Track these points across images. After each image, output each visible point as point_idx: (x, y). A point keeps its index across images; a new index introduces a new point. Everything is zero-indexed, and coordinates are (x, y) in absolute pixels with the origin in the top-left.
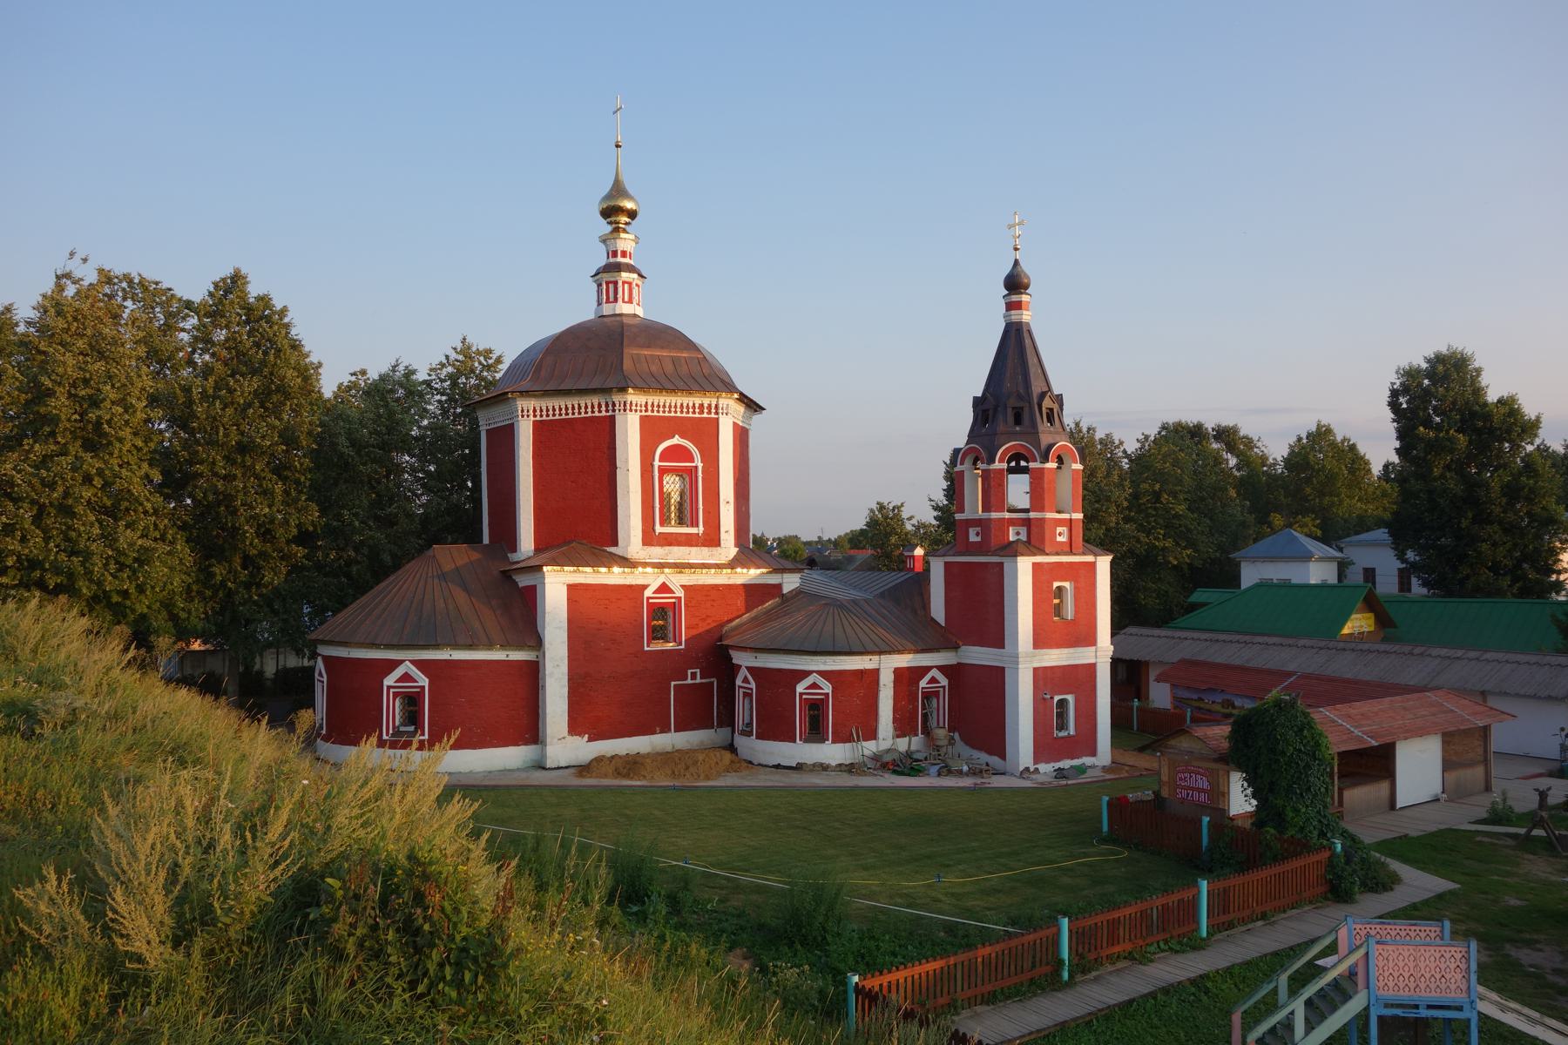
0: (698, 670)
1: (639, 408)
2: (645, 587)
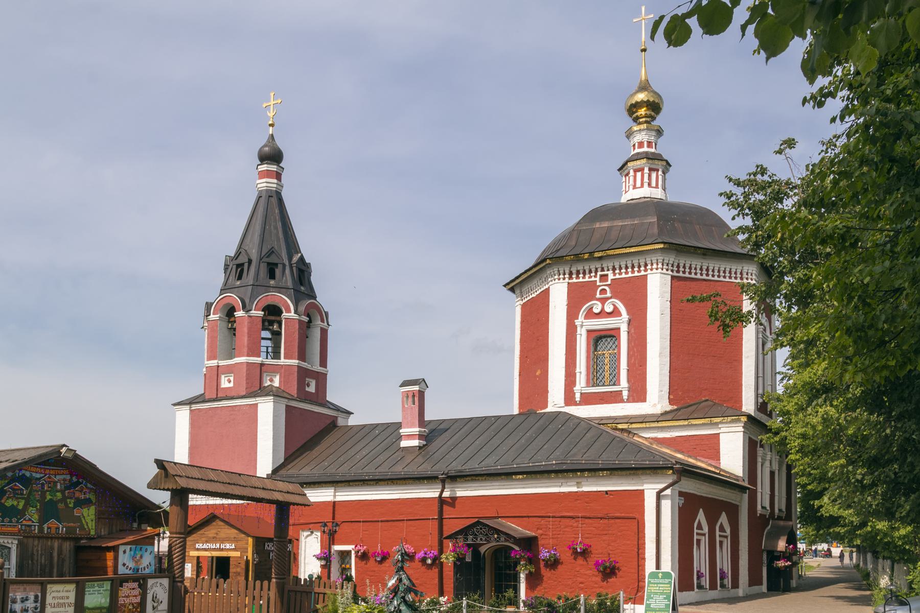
1: (670, 267)
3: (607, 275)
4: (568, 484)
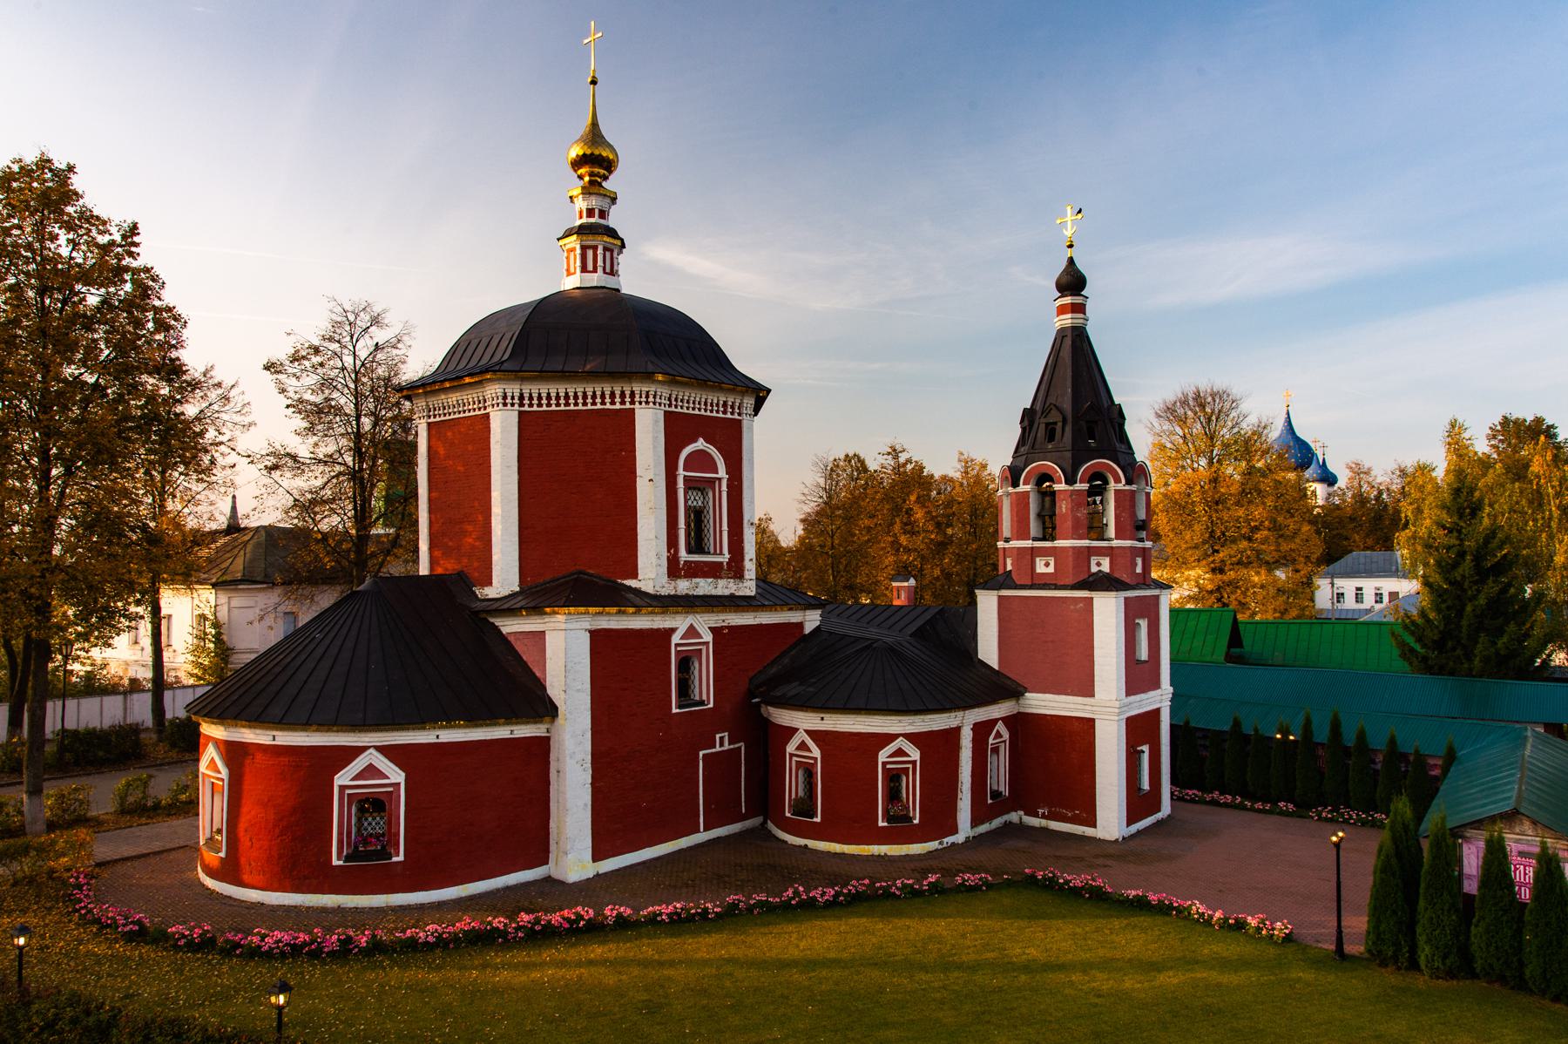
0: (726, 734)
2: (673, 630)
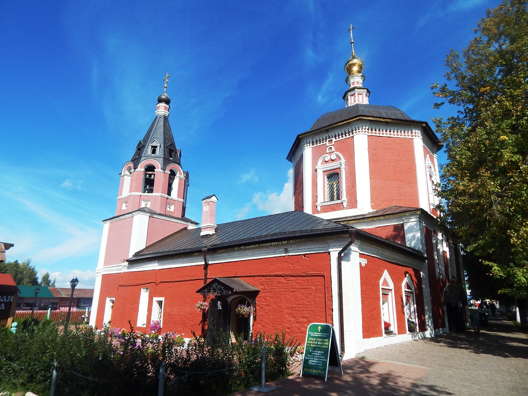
3: (332, 140)
4: (279, 250)
